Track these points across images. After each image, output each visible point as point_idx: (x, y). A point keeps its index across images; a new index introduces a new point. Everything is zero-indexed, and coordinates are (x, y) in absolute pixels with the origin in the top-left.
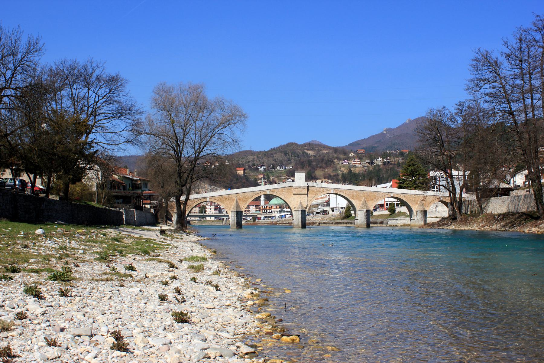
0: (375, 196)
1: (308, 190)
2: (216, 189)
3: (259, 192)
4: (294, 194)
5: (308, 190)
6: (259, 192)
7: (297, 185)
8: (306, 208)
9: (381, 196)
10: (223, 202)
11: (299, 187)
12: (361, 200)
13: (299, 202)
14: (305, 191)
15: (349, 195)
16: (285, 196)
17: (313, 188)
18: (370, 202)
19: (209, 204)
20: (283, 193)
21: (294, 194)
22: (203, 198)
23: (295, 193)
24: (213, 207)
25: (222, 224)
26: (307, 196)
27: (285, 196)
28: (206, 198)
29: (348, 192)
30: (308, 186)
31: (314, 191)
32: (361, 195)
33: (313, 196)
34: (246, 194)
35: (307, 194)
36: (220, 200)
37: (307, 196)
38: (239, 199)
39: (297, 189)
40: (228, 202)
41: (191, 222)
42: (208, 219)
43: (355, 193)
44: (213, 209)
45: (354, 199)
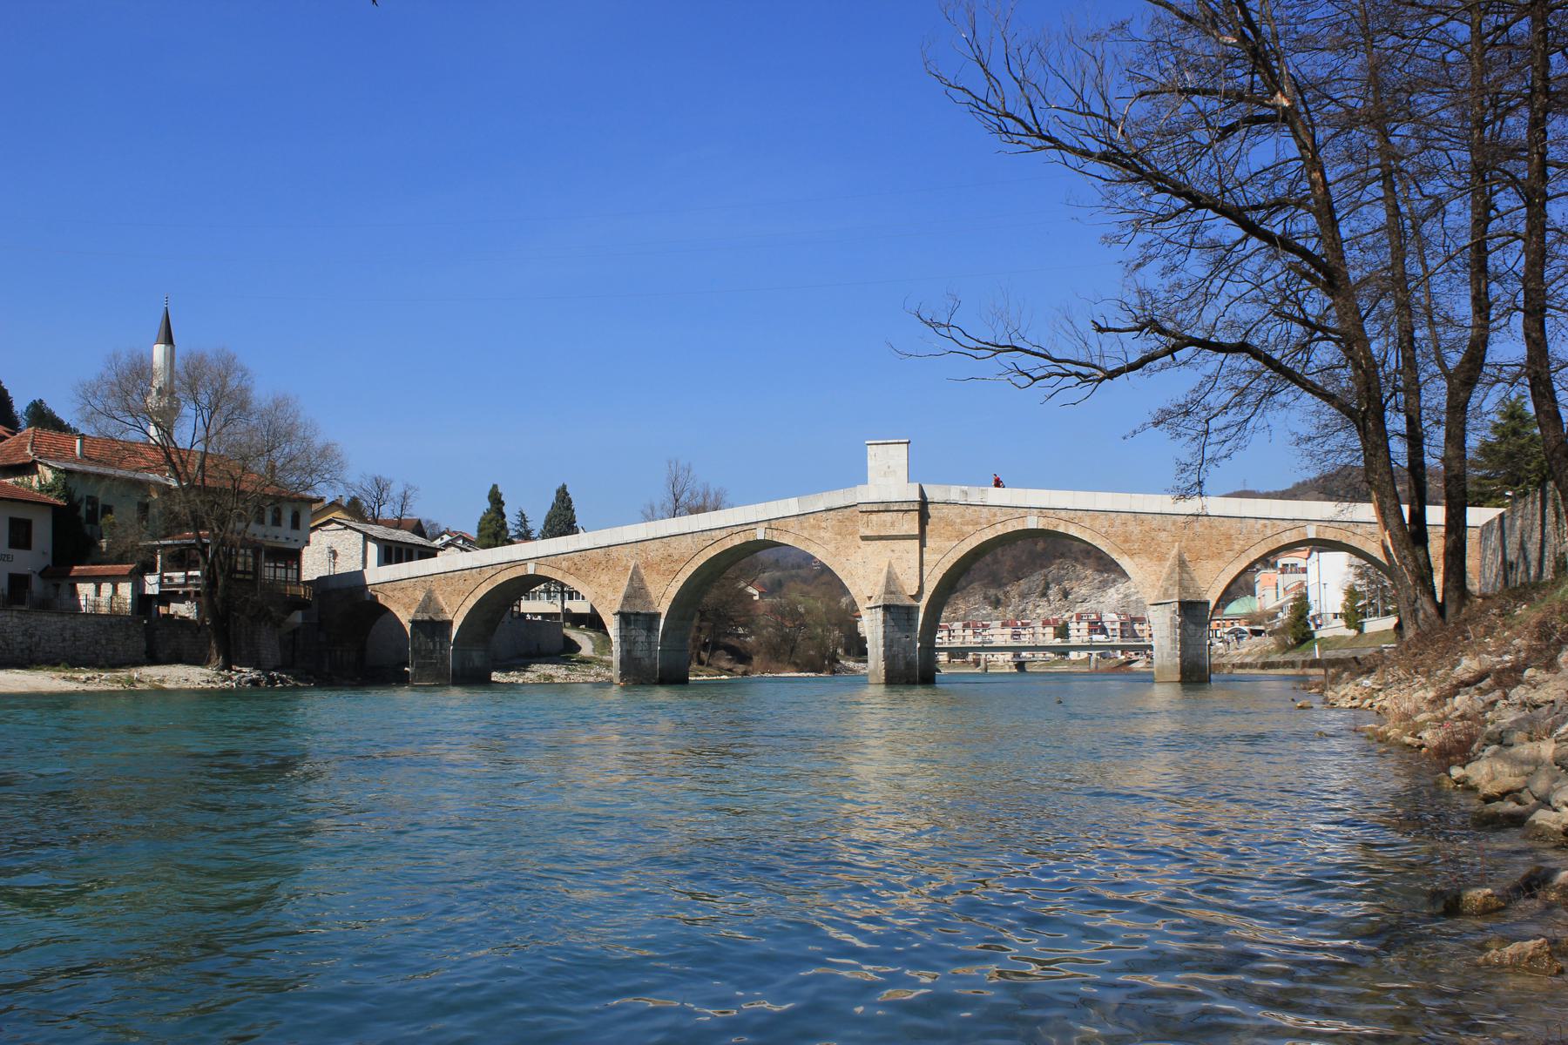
0: (1229, 537)
1: (924, 518)
2: (1114, 581)
3: (724, 533)
4: (865, 538)
5: (924, 518)
6: (724, 533)
7: (874, 497)
8: (917, 596)
9: (1257, 538)
10: (585, 578)
11: (885, 508)
12: (1162, 559)
13: (885, 571)
14: (911, 525)
15: (1107, 536)
16: (831, 547)
17: (946, 510)
18: (1209, 565)
19: (1074, 619)
20: (822, 534)
21: (865, 538)
22: (513, 563)
23: (868, 533)
24: (1085, 625)
25: (1087, 670)
26: (923, 545)
27: (831, 547)
28: (523, 562)
29: (1102, 523)
30: (924, 504)
31: (952, 523)
32: (1163, 535)
33: (949, 545)
34: (674, 542)
35: (922, 538)
36: (576, 570)
37: (923, 545)
38: (648, 565)
39: (874, 517)
40: (604, 579)
41: (1026, 665)
42: (1073, 655)
43: (1135, 529)
44: (1084, 632)
45: (1131, 555)
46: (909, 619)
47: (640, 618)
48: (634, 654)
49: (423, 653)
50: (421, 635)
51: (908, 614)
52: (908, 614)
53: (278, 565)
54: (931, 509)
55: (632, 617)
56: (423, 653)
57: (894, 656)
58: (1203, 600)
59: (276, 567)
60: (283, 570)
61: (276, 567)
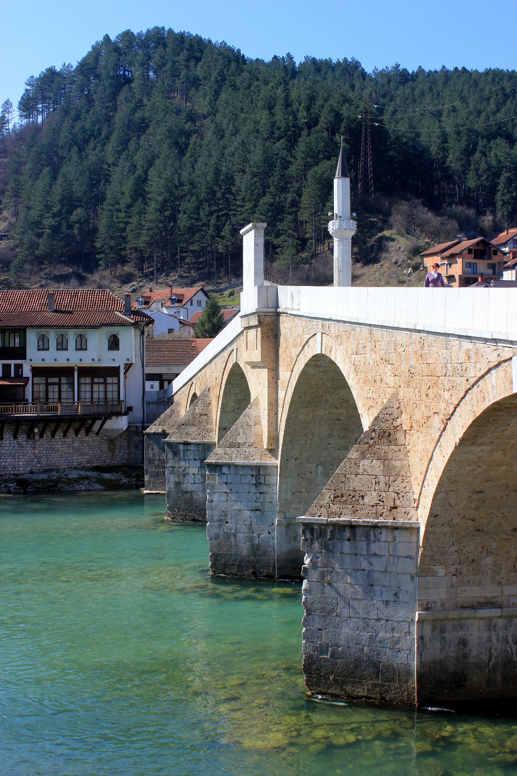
8: (272, 451)
46: (258, 484)
47: (191, 448)
48: (184, 487)
49: (156, 463)
50: (155, 447)
51: (257, 477)
52: (257, 477)
53: (96, 380)
54: (285, 324)
55: (181, 447)
56: (156, 463)
57: (227, 536)
58: (400, 521)
59: (92, 383)
60: (102, 388)
61: (92, 383)
